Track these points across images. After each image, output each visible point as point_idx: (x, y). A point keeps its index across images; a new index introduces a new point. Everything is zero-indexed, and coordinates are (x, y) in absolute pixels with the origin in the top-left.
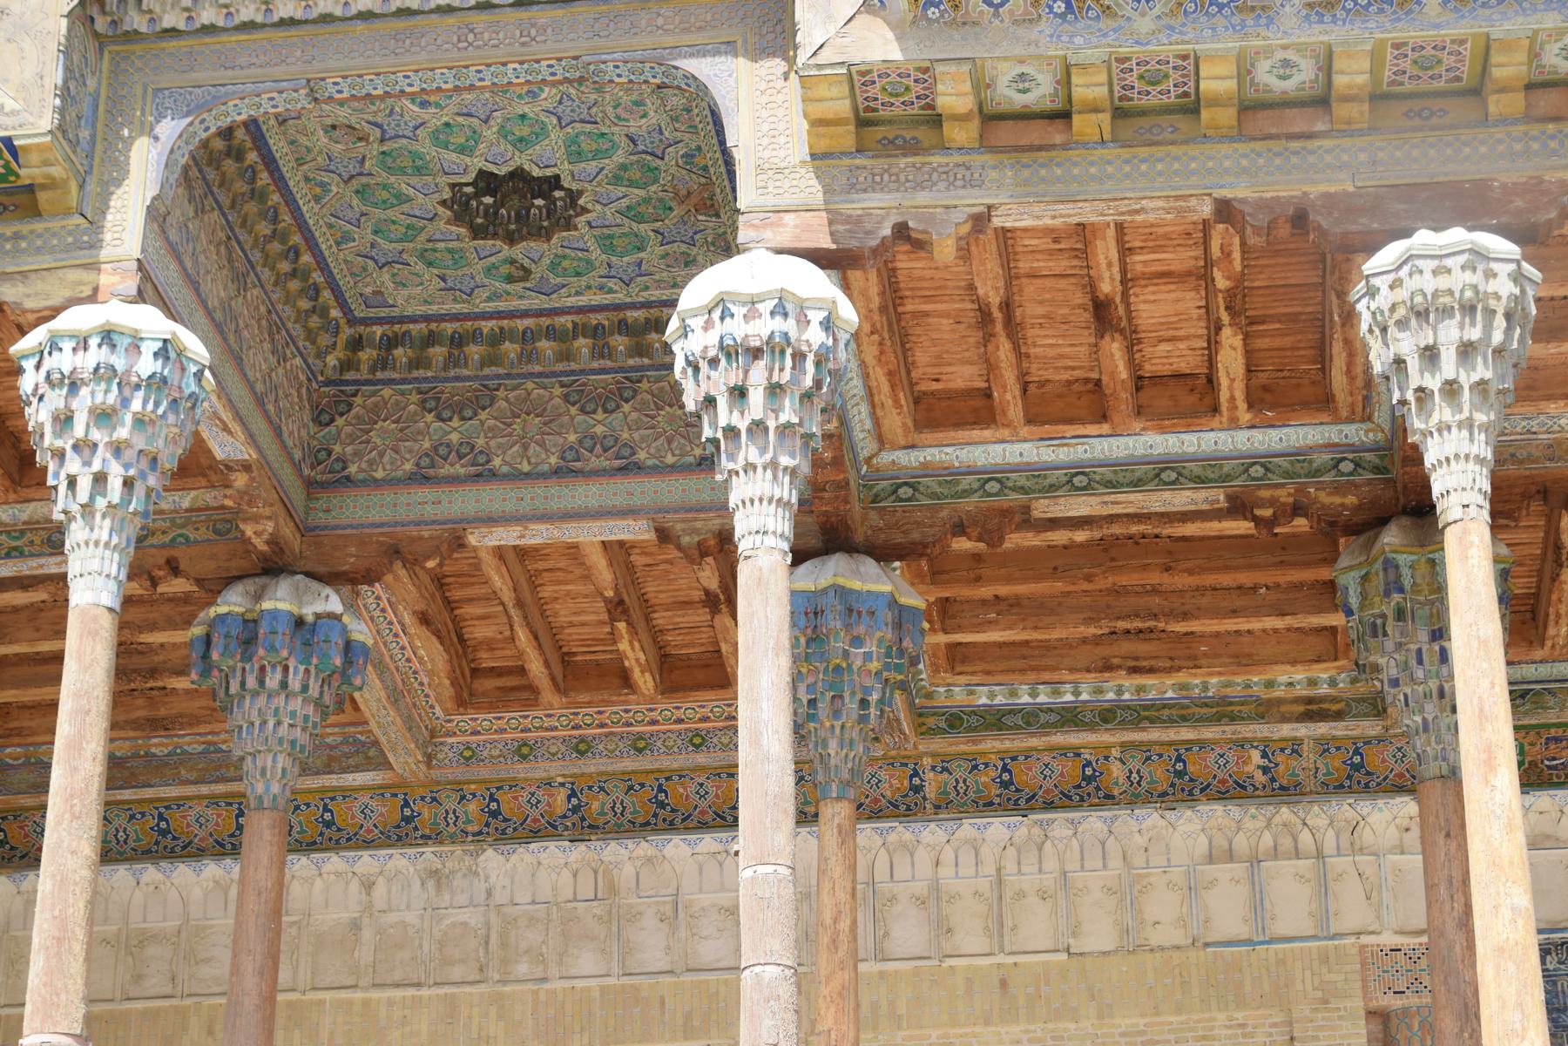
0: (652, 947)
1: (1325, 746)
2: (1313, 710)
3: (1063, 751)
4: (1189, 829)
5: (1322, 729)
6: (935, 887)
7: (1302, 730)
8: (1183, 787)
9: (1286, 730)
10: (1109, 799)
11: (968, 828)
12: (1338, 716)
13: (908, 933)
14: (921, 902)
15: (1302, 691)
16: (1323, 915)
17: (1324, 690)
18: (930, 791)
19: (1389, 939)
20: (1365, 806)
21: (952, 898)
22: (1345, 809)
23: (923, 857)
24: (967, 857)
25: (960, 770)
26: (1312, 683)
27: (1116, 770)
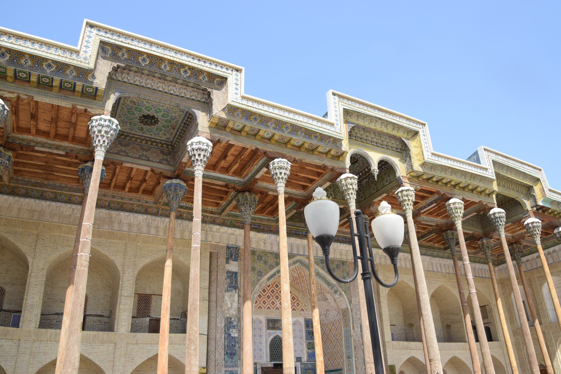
0: (116, 227)
1: (211, 217)
2: (212, 213)
3: (179, 211)
5: (212, 215)
6: (157, 226)
7: (210, 215)
9: (208, 214)
10: (183, 219)
11: (163, 219)
13: (153, 231)
14: (155, 227)
16: (206, 238)
18: (160, 213)
19: (213, 243)
20: (213, 226)
21: (160, 228)
22: (211, 226)
23: (156, 222)
24: (162, 223)
25: (165, 211)
27: (185, 215)
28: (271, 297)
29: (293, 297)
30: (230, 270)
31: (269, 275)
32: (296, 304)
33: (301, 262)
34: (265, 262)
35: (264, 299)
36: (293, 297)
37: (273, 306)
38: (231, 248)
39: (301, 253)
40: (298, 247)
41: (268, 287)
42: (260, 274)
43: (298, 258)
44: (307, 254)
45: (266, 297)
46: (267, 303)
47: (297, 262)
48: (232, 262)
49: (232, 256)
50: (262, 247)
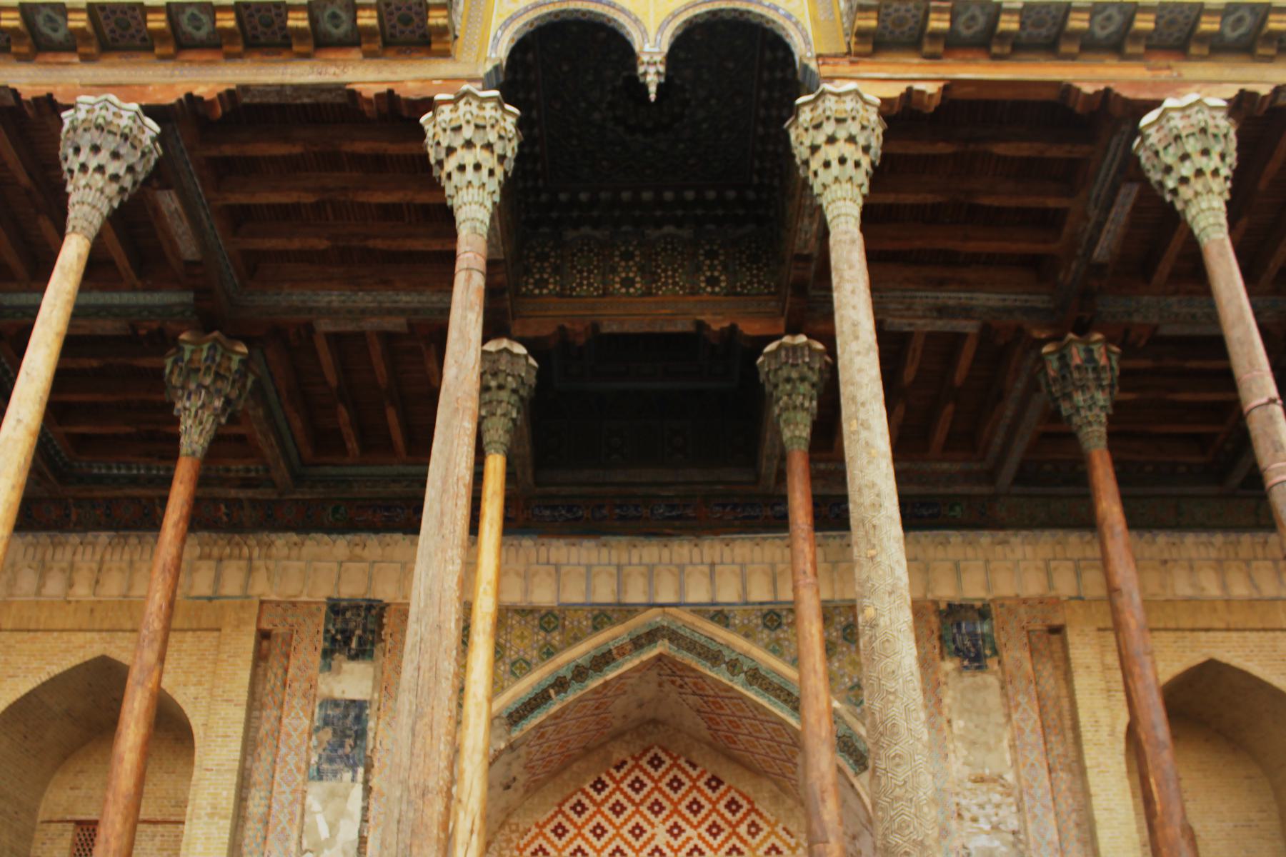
2: (246, 483)
5: (250, 493)
12: (257, 487)
15: (242, 474)
17: (253, 474)
26: (248, 470)
28: (631, 809)
29: (733, 801)
30: (337, 694)
32: (742, 830)
33: (674, 637)
35: (599, 818)
36: (733, 801)
37: (637, 845)
38: (345, 610)
39: (666, 596)
41: (618, 768)
43: (652, 617)
45: (605, 809)
46: (611, 831)
47: (652, 635)
48: (349, 666)
49: (347, 641)
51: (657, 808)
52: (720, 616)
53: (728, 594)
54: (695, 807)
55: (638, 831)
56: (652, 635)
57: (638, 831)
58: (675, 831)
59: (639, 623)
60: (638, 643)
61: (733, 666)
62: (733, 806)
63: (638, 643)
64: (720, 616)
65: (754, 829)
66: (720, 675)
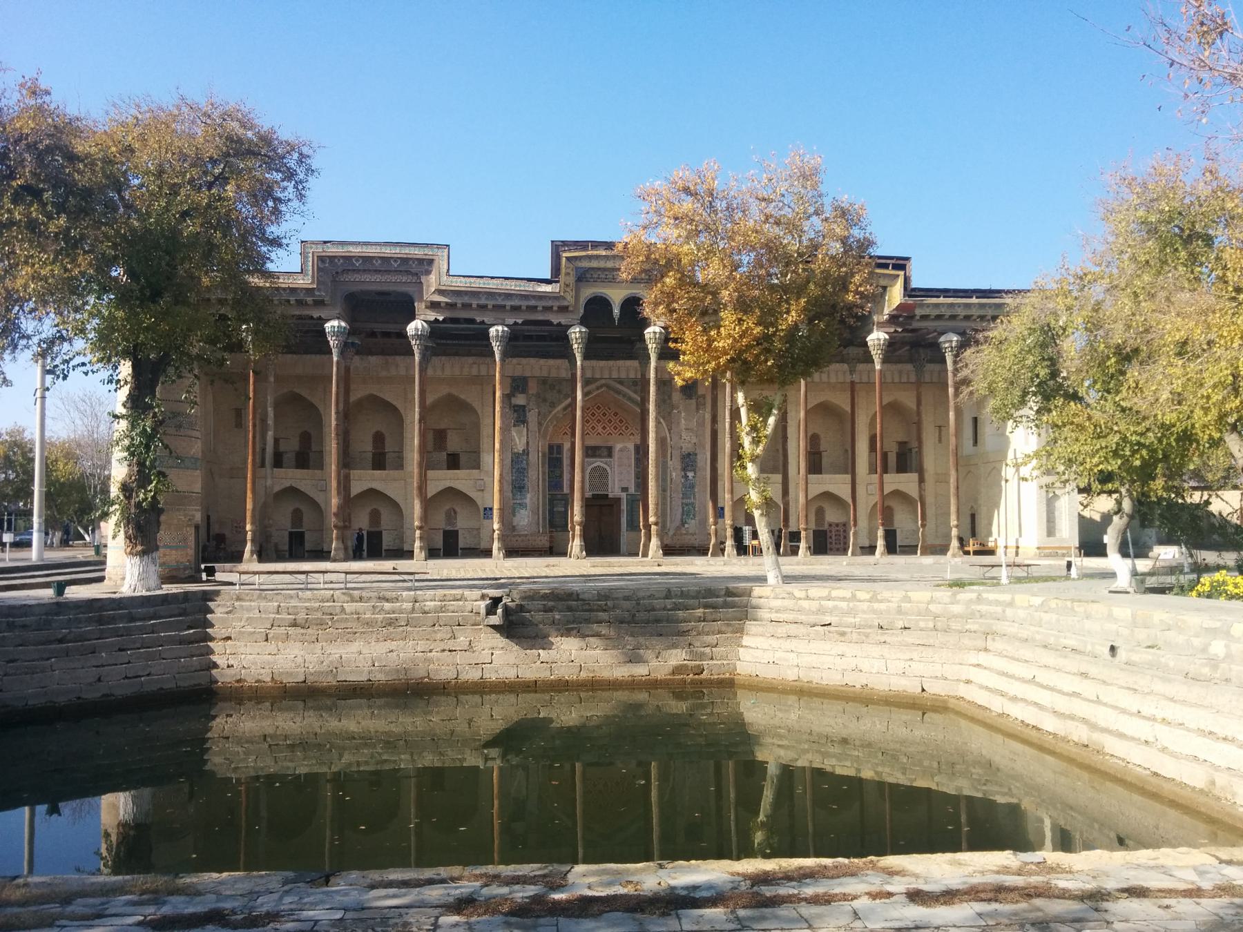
4: (470, 360)
8: (469, 354)
31: (563, 405)
33: (608, 386)
34: (559, 392)
40: (602, 369)
42: (553, 405)
43: (603, 382)
44: (615, 375)
47: (601, 386)
50: (554, 374)
51: (599, 421)
52: (621, 382)
53: (623, 376)
54: (610, 421)
55: (593, 428)
56: (601, 386)
57: (593, 428)
58: (604, 428)
59: (598, 384)
60: (598, 388)
61: (624, 396)
62: (621, 421)
63: (598, 388)
64: (621, 382)
65: (627, 428)
66: (620, 397)
